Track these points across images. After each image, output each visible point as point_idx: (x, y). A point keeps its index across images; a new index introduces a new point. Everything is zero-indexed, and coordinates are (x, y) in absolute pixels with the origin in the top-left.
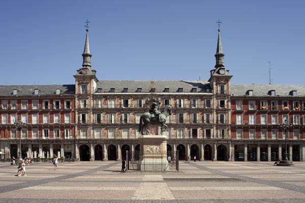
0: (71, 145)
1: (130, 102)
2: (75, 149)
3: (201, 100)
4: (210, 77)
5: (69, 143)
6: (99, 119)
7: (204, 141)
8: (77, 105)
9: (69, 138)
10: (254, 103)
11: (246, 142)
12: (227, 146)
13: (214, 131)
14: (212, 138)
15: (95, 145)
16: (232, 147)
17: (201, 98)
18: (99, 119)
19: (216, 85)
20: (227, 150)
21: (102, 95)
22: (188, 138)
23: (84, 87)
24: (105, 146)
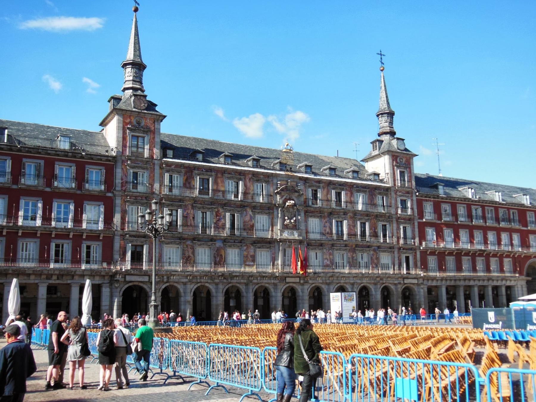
7: (382, 279)
8: (118, 181)
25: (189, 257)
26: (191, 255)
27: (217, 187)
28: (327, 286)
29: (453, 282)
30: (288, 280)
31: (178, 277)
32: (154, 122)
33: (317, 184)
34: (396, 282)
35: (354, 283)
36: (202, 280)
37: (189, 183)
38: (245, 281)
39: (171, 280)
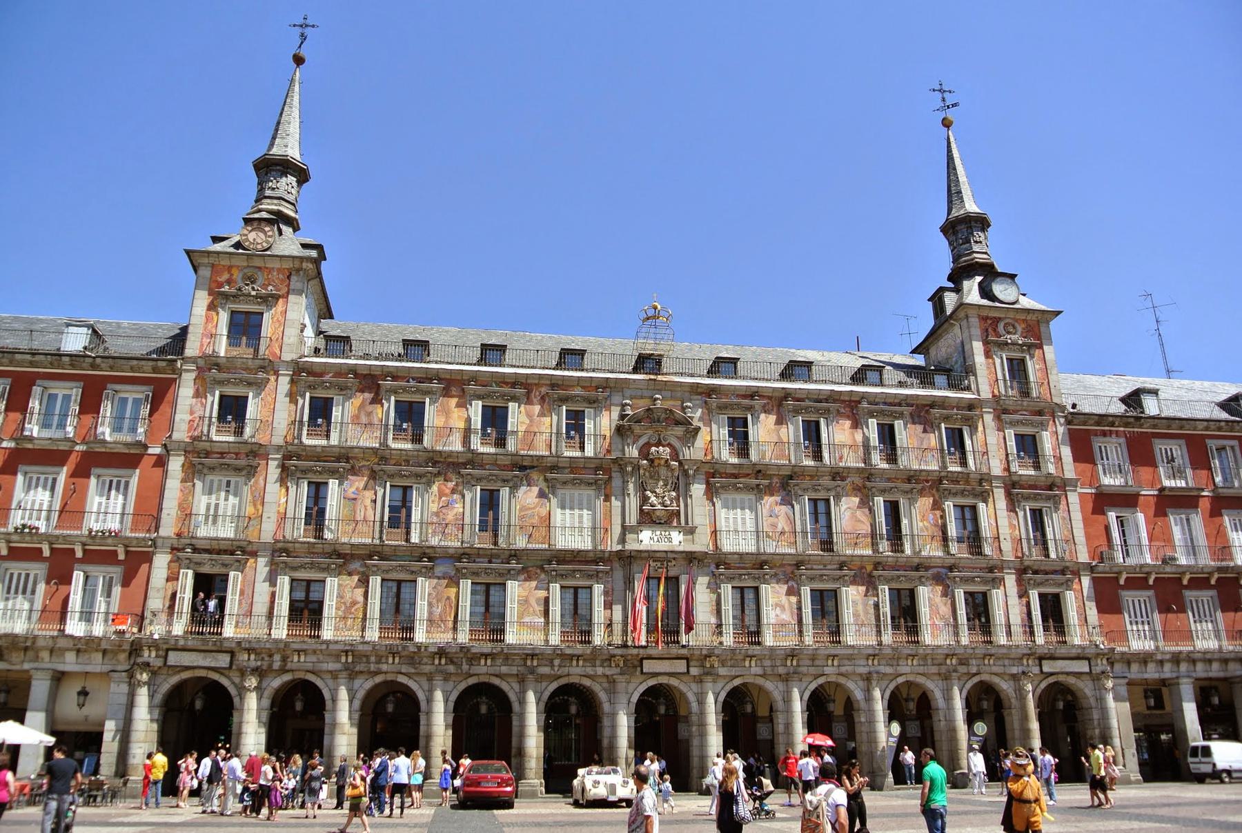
0: (106, 675)
1: (517, 416)
2: (131, 705)
3: (925, 431)
4: (928, 322)
5: (96, 664)
6: (316, 516)
7: (963, 662)
8: (182, 417)
9: (98, 630)
10: (1178, 450)
11: (1184, 667)
12: (1086, 688)
13: (1007, 603)
14: (1002, 640)
15: (276, 683)
16: (1117, 699)
17: (922, 413)
18: (316, 516)
19: (988, 355)
20: (1096, 715)
21: (353, 370)
22: (872, 641)
23: (245, 327)
24: (343, 694)
25: (354, 603)
26: (361, 599)
27: (446, 422)
28: (781, 686)
29: (1215, 666)
30: (648, 666)
31: (314, 659)
32: (289, 277)
33: (747, 402)
34: (1014, 670)
35: (870, 673)
36: (384, 667)
37: (369, 414)
38: (514, 670)
39: (294, 666)
